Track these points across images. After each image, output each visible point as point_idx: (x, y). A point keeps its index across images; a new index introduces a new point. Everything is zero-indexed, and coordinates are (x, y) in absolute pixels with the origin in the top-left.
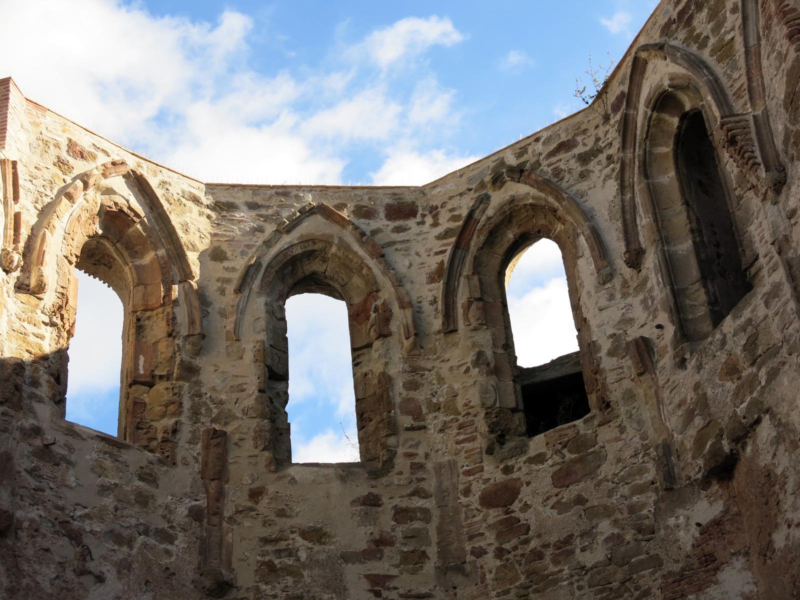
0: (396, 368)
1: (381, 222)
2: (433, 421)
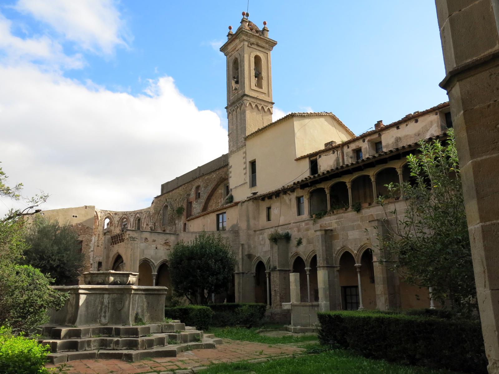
0: (113, 229)
1: (114, 215)
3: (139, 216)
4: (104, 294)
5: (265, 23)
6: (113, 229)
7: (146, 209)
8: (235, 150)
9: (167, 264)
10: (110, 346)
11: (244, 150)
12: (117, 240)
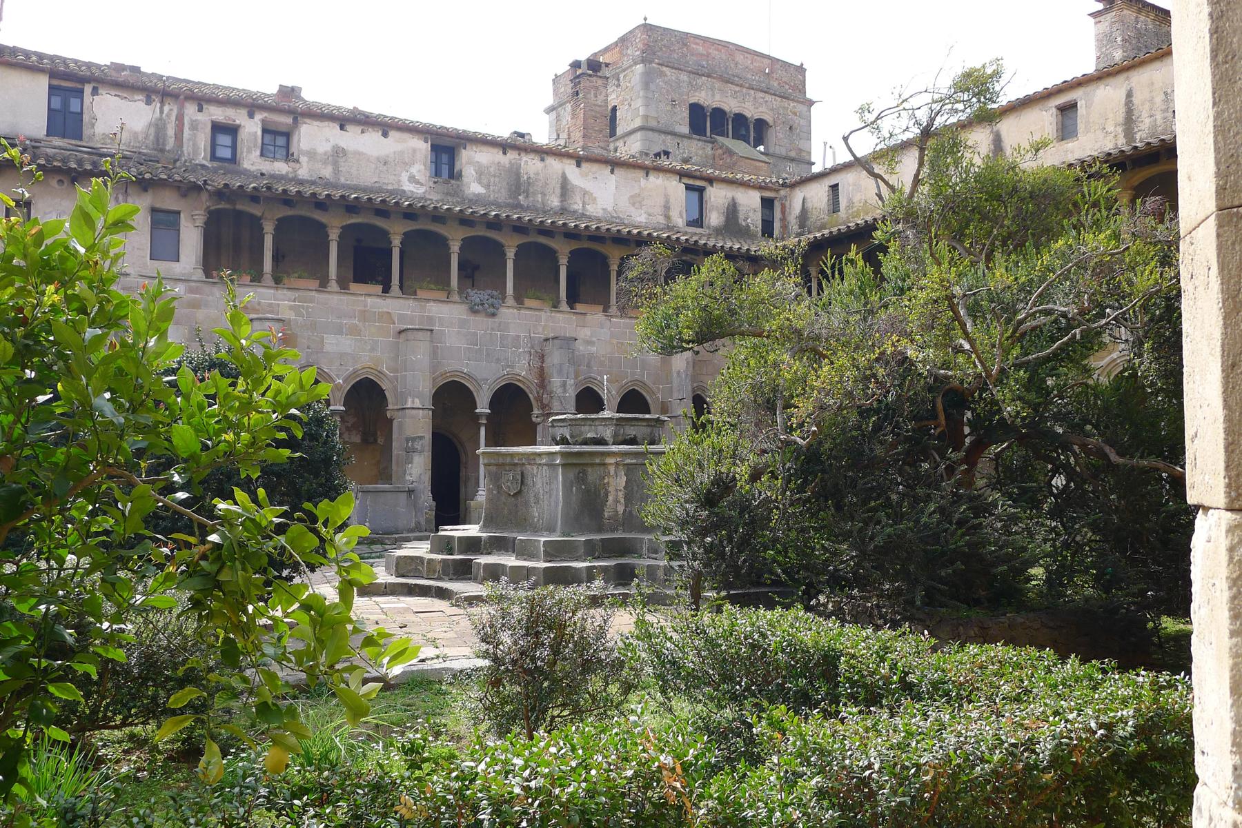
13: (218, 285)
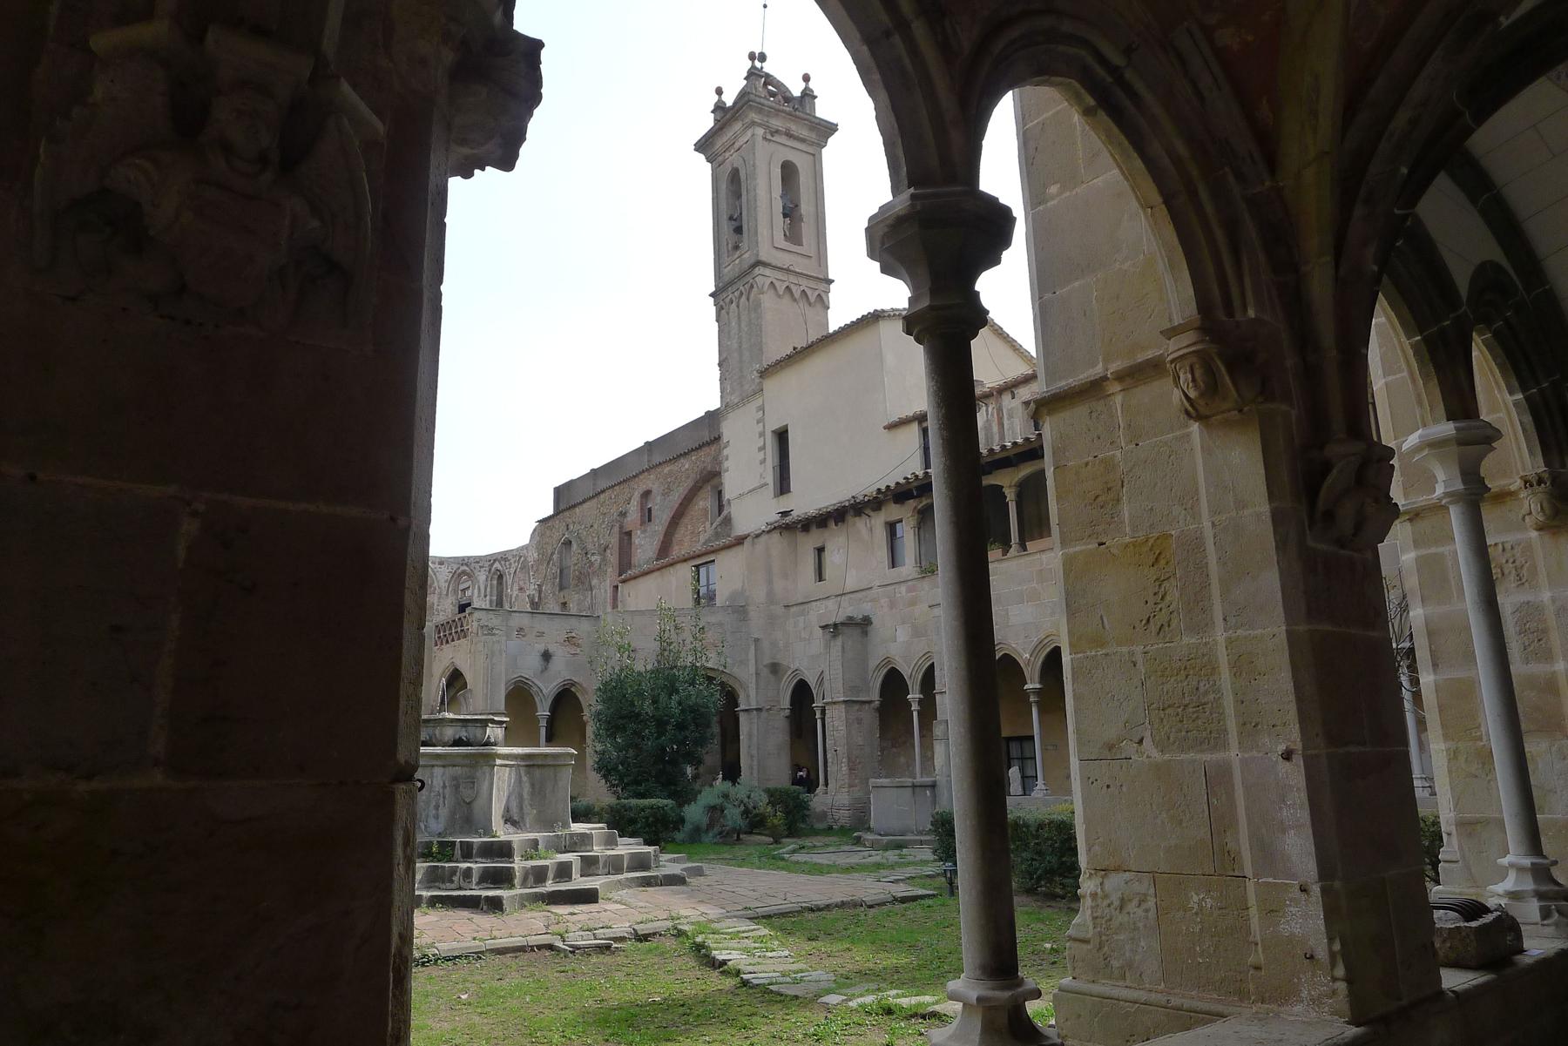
0: (436, 602)
1: (437, 565)
2: (441, 613)
3: (500, 568)
4: (433, 766)
5: (806, 78)
6: (436, 602)
7: (517, 550)
8: (736, 401)
9: (573, 689)
10: (452, 882)
11: (759, 402)
12: (451, 634)
13: (926, 579)
